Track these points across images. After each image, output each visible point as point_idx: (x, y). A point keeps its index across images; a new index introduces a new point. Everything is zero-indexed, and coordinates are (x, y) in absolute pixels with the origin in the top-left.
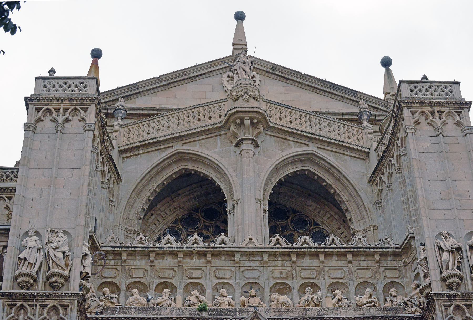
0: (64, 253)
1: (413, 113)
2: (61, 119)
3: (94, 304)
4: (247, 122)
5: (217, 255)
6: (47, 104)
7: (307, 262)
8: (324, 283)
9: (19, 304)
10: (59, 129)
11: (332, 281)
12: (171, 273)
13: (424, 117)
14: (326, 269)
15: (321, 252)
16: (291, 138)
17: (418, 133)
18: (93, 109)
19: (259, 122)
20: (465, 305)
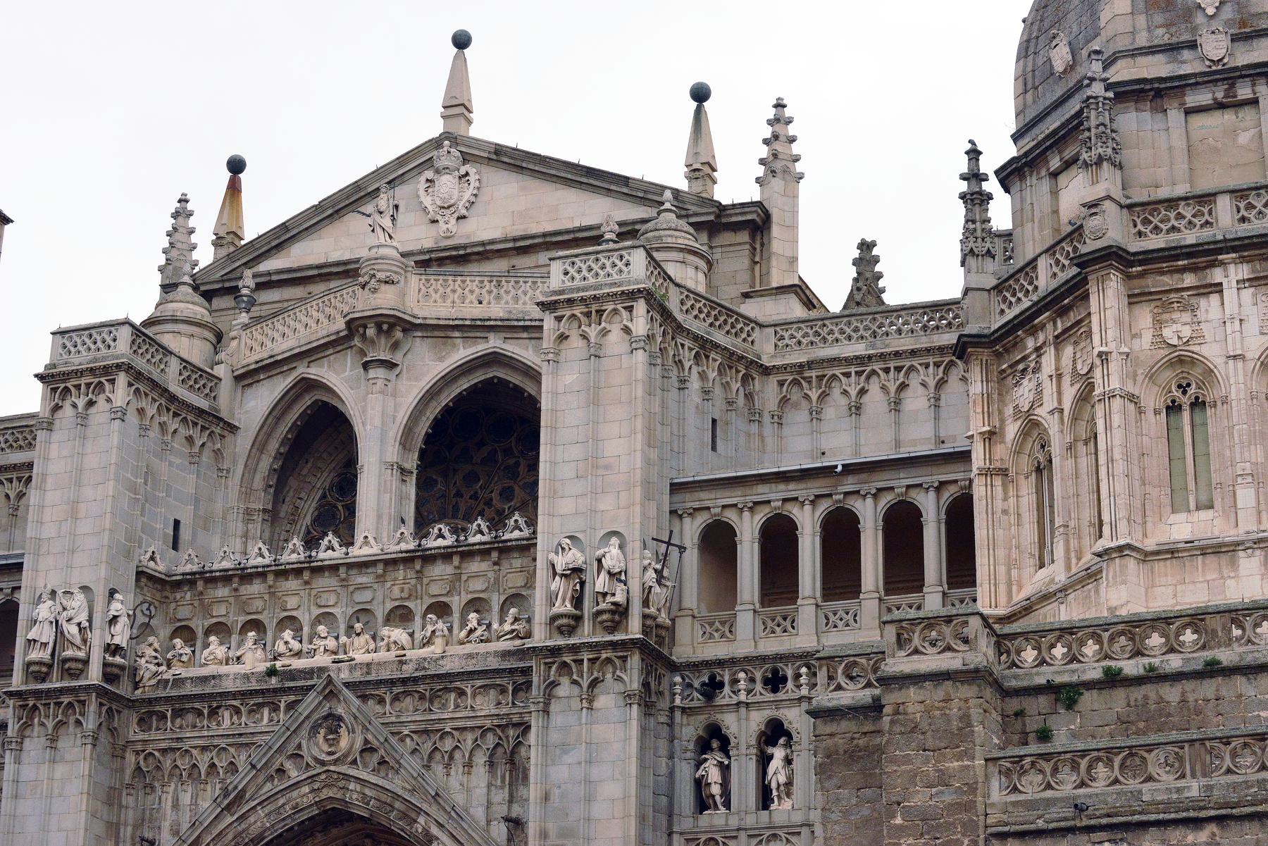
0: (79, 624)
1: (559, 319)
2: (81, 403)
3: (147, 675)
4: (371, 332)
5: (318, 570)
6: (64, 381)
7: (440, 570)
8: (456, 603)
9: (31, 703)
10: (83, 419)
11: (470, 596)
12: (258, 604)
13: (575, 324)
14: (464, 577)
15: (456, 553)
16: (457, 334)
17: (562, 358)
18: (122, 379)
19: (392, 327)
20: (575, 661)
